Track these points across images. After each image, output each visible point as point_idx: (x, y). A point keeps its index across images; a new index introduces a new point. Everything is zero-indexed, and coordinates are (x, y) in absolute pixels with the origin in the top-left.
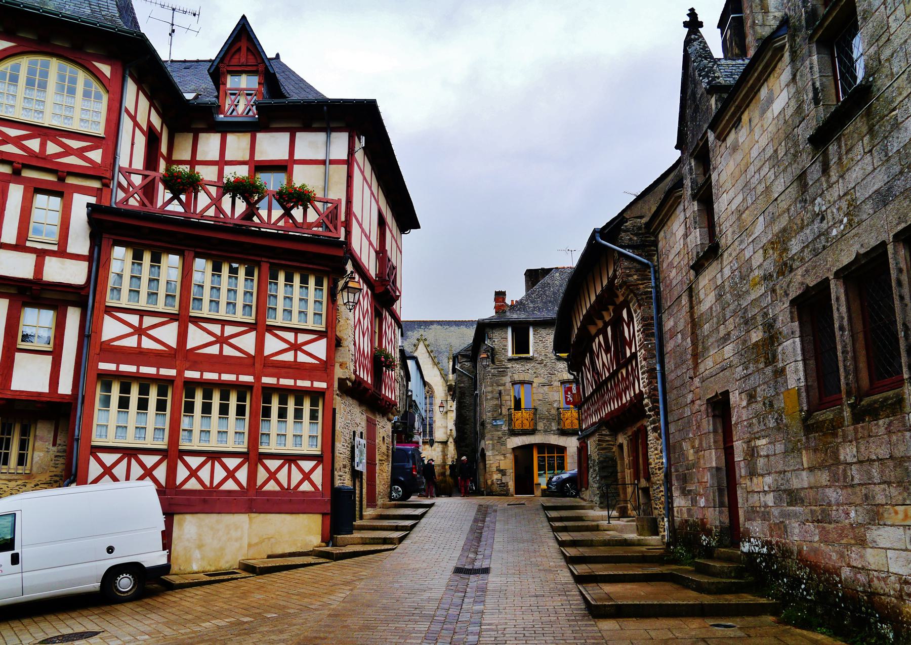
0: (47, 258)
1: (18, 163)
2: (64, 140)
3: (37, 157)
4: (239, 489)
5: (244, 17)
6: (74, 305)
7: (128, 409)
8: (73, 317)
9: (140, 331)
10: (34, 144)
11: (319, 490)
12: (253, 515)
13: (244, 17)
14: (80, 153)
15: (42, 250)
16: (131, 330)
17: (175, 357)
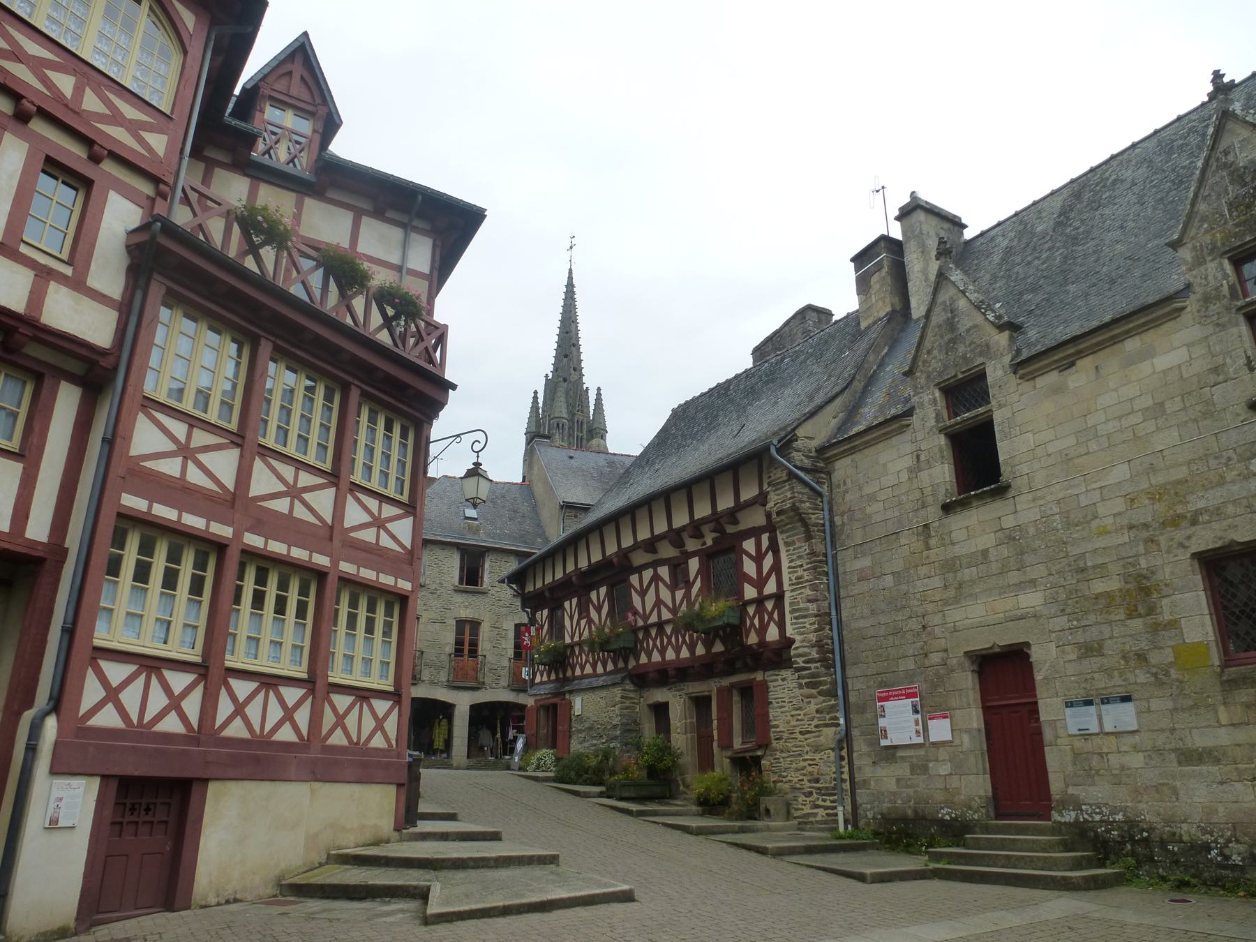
0: (53, 285)
1: (33, 103)
2: (112, 97)
3: (66, 106)
4: (298, 741)
5: (305, 34)
6: (73, 379)
7: (147, 584)
8: (67, 401)
9: (186, 452)
10: (65, 83)
11: (392, 746)
12: (317, 785)
13: (305, 34)
14: (134, 128)
15: (45, 266)
16: (171, 447)
17: (233, 507)
